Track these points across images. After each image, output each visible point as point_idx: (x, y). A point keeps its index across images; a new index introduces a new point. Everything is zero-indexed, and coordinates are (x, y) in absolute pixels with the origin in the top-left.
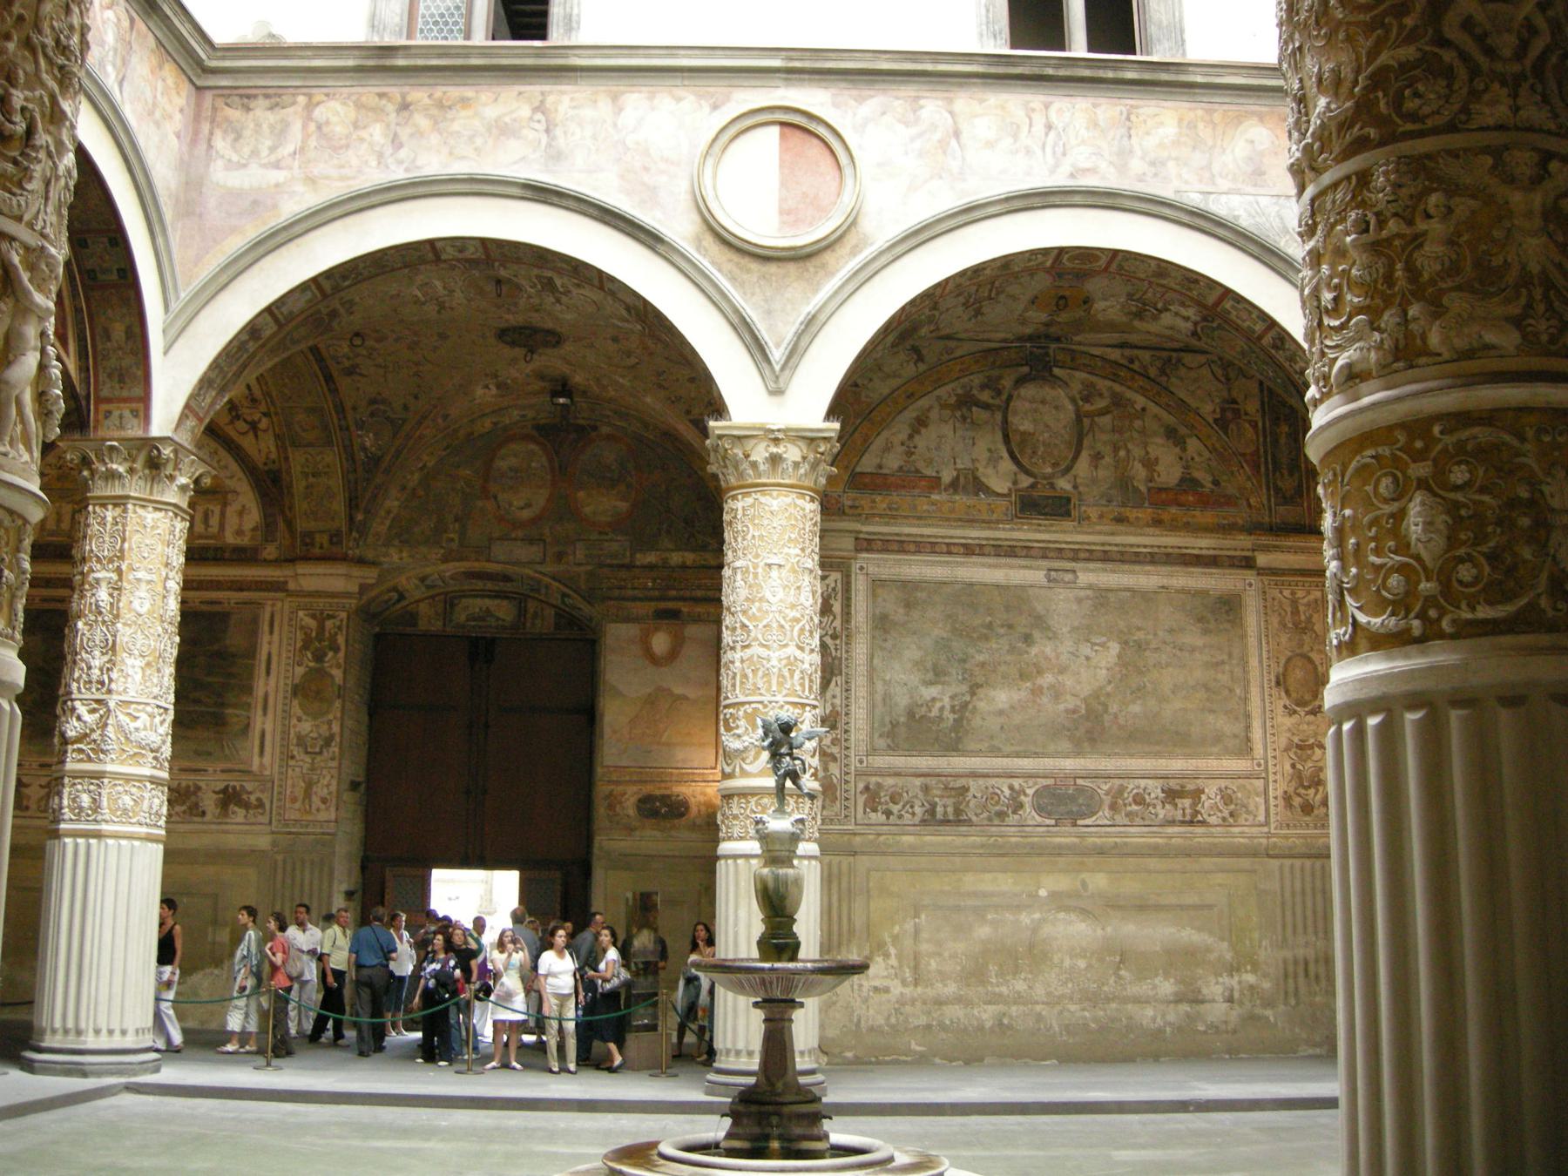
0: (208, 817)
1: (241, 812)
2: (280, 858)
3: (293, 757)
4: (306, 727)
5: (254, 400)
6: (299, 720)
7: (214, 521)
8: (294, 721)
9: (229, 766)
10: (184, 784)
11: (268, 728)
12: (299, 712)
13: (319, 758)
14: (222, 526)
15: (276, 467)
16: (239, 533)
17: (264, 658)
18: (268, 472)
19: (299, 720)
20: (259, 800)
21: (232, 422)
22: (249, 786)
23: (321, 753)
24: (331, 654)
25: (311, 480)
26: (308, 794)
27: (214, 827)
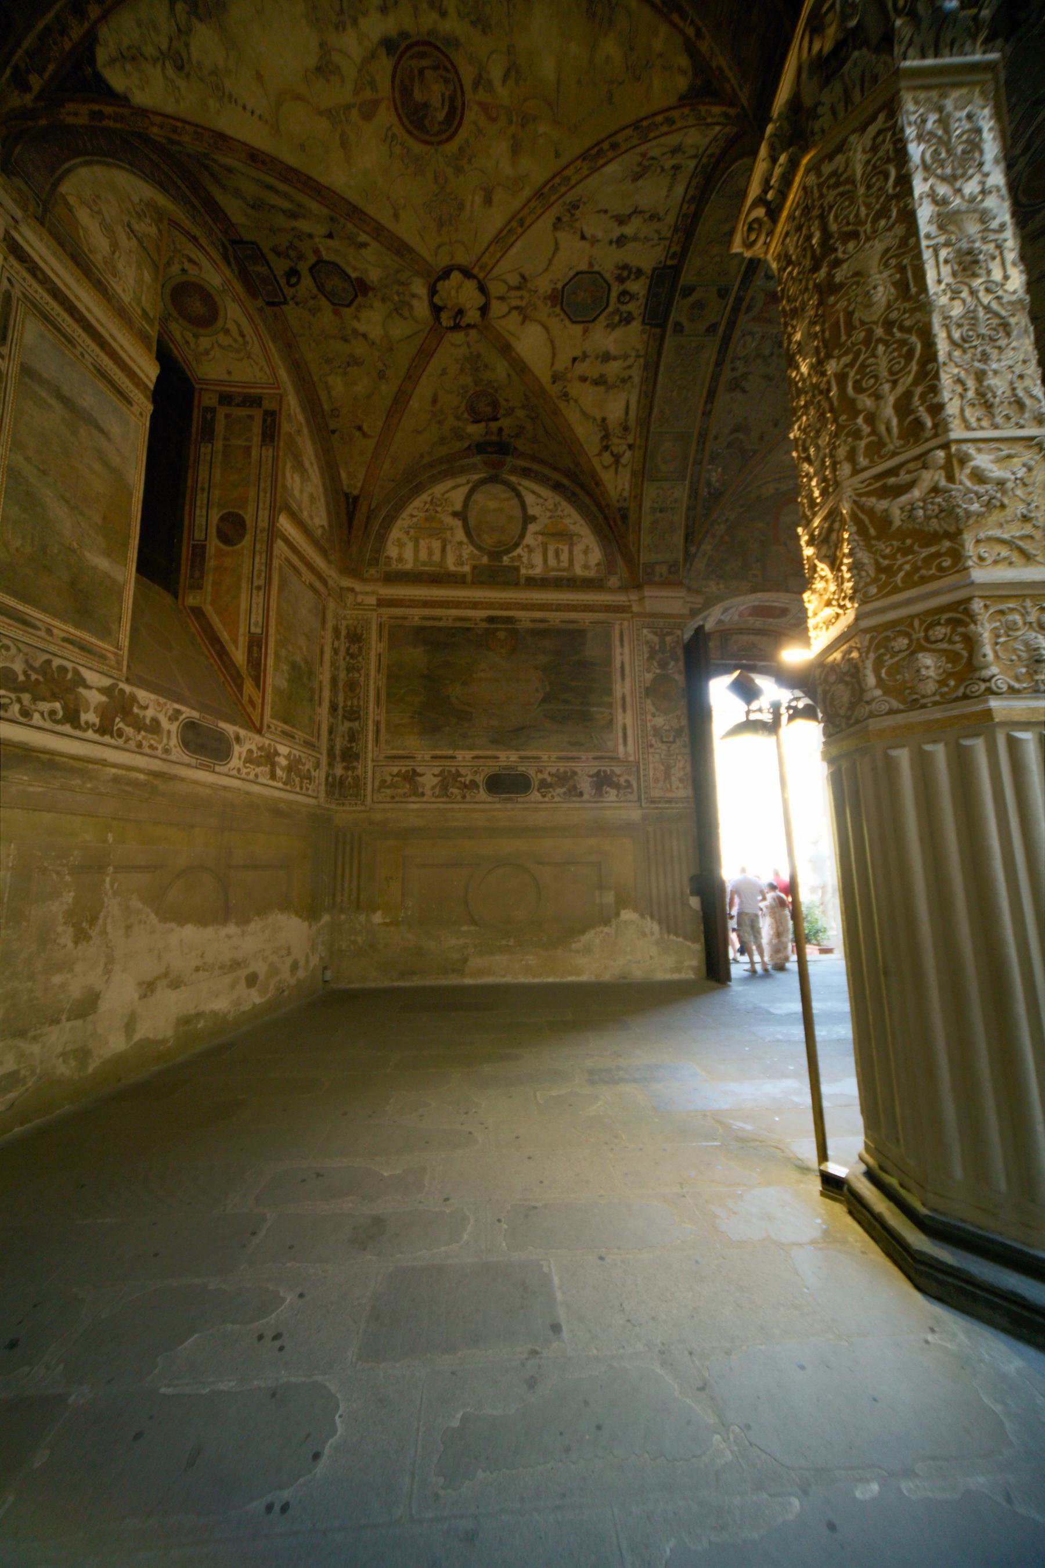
0: (586, 797)
1: (613, 792)
2: (650, 829)
3: (652, 746)
4: (659, 721)
5: (626, 429)
6: (654, 715)
7: (564, 557)
8: (649, 717)
9: (599, 754)
10: (562, 770)
11: (629, 722)
12: (653, 710)
13: (673, 747)
14: (571, 562)
15: (625, 505)
16: (586, 567)
17: (618, 665)
18: (620, 510)
19: (654, 715)
20: (627, 781)
21: (600, 454)
22: (618, 770)
23: (674, 742)
24: (672, 663)
25: (658, 515)
26: (667, 776)
27: (590, 805)
